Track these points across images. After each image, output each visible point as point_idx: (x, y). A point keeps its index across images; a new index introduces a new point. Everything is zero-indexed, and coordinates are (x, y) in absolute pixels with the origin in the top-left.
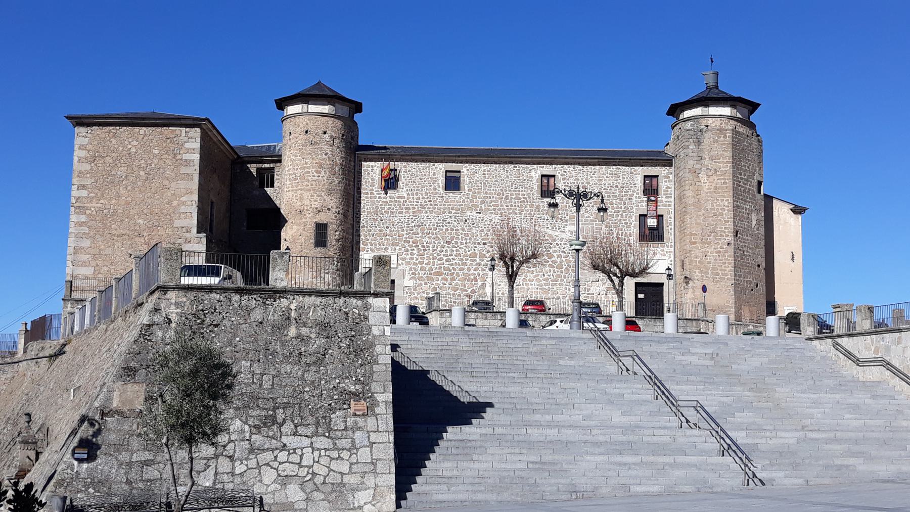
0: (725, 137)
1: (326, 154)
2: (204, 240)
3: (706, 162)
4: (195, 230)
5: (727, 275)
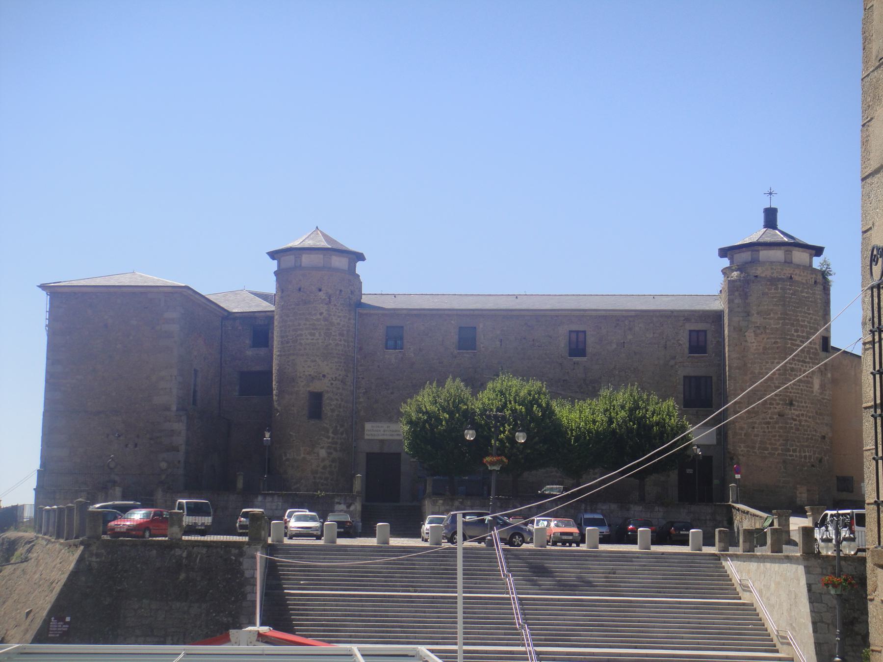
0: (776, 289)
1: (321, 314)
2: (184, 418)
3: (756, 319)
4: (174, 408)
5: (776, 449)
